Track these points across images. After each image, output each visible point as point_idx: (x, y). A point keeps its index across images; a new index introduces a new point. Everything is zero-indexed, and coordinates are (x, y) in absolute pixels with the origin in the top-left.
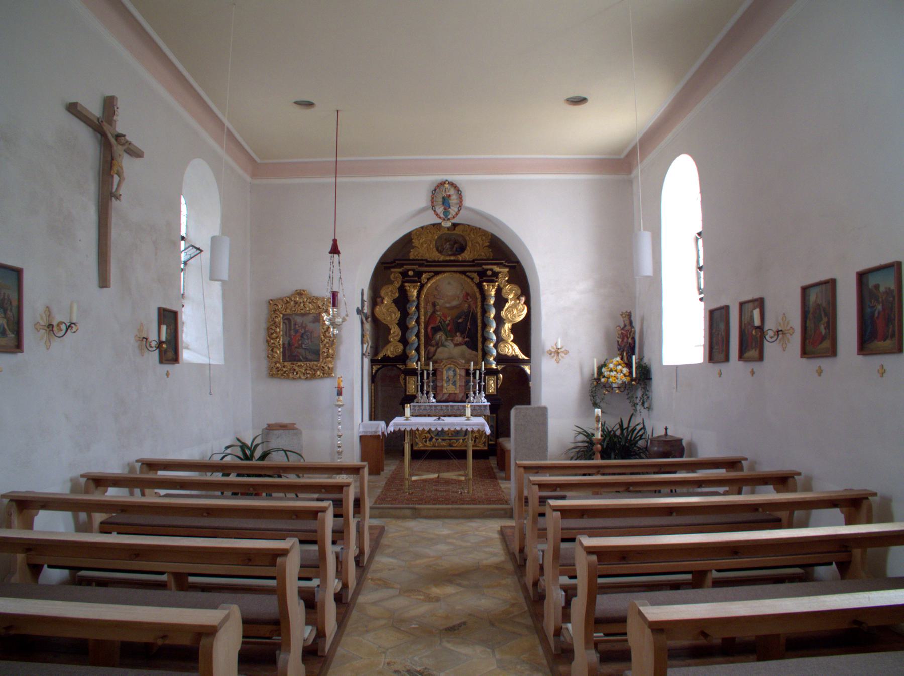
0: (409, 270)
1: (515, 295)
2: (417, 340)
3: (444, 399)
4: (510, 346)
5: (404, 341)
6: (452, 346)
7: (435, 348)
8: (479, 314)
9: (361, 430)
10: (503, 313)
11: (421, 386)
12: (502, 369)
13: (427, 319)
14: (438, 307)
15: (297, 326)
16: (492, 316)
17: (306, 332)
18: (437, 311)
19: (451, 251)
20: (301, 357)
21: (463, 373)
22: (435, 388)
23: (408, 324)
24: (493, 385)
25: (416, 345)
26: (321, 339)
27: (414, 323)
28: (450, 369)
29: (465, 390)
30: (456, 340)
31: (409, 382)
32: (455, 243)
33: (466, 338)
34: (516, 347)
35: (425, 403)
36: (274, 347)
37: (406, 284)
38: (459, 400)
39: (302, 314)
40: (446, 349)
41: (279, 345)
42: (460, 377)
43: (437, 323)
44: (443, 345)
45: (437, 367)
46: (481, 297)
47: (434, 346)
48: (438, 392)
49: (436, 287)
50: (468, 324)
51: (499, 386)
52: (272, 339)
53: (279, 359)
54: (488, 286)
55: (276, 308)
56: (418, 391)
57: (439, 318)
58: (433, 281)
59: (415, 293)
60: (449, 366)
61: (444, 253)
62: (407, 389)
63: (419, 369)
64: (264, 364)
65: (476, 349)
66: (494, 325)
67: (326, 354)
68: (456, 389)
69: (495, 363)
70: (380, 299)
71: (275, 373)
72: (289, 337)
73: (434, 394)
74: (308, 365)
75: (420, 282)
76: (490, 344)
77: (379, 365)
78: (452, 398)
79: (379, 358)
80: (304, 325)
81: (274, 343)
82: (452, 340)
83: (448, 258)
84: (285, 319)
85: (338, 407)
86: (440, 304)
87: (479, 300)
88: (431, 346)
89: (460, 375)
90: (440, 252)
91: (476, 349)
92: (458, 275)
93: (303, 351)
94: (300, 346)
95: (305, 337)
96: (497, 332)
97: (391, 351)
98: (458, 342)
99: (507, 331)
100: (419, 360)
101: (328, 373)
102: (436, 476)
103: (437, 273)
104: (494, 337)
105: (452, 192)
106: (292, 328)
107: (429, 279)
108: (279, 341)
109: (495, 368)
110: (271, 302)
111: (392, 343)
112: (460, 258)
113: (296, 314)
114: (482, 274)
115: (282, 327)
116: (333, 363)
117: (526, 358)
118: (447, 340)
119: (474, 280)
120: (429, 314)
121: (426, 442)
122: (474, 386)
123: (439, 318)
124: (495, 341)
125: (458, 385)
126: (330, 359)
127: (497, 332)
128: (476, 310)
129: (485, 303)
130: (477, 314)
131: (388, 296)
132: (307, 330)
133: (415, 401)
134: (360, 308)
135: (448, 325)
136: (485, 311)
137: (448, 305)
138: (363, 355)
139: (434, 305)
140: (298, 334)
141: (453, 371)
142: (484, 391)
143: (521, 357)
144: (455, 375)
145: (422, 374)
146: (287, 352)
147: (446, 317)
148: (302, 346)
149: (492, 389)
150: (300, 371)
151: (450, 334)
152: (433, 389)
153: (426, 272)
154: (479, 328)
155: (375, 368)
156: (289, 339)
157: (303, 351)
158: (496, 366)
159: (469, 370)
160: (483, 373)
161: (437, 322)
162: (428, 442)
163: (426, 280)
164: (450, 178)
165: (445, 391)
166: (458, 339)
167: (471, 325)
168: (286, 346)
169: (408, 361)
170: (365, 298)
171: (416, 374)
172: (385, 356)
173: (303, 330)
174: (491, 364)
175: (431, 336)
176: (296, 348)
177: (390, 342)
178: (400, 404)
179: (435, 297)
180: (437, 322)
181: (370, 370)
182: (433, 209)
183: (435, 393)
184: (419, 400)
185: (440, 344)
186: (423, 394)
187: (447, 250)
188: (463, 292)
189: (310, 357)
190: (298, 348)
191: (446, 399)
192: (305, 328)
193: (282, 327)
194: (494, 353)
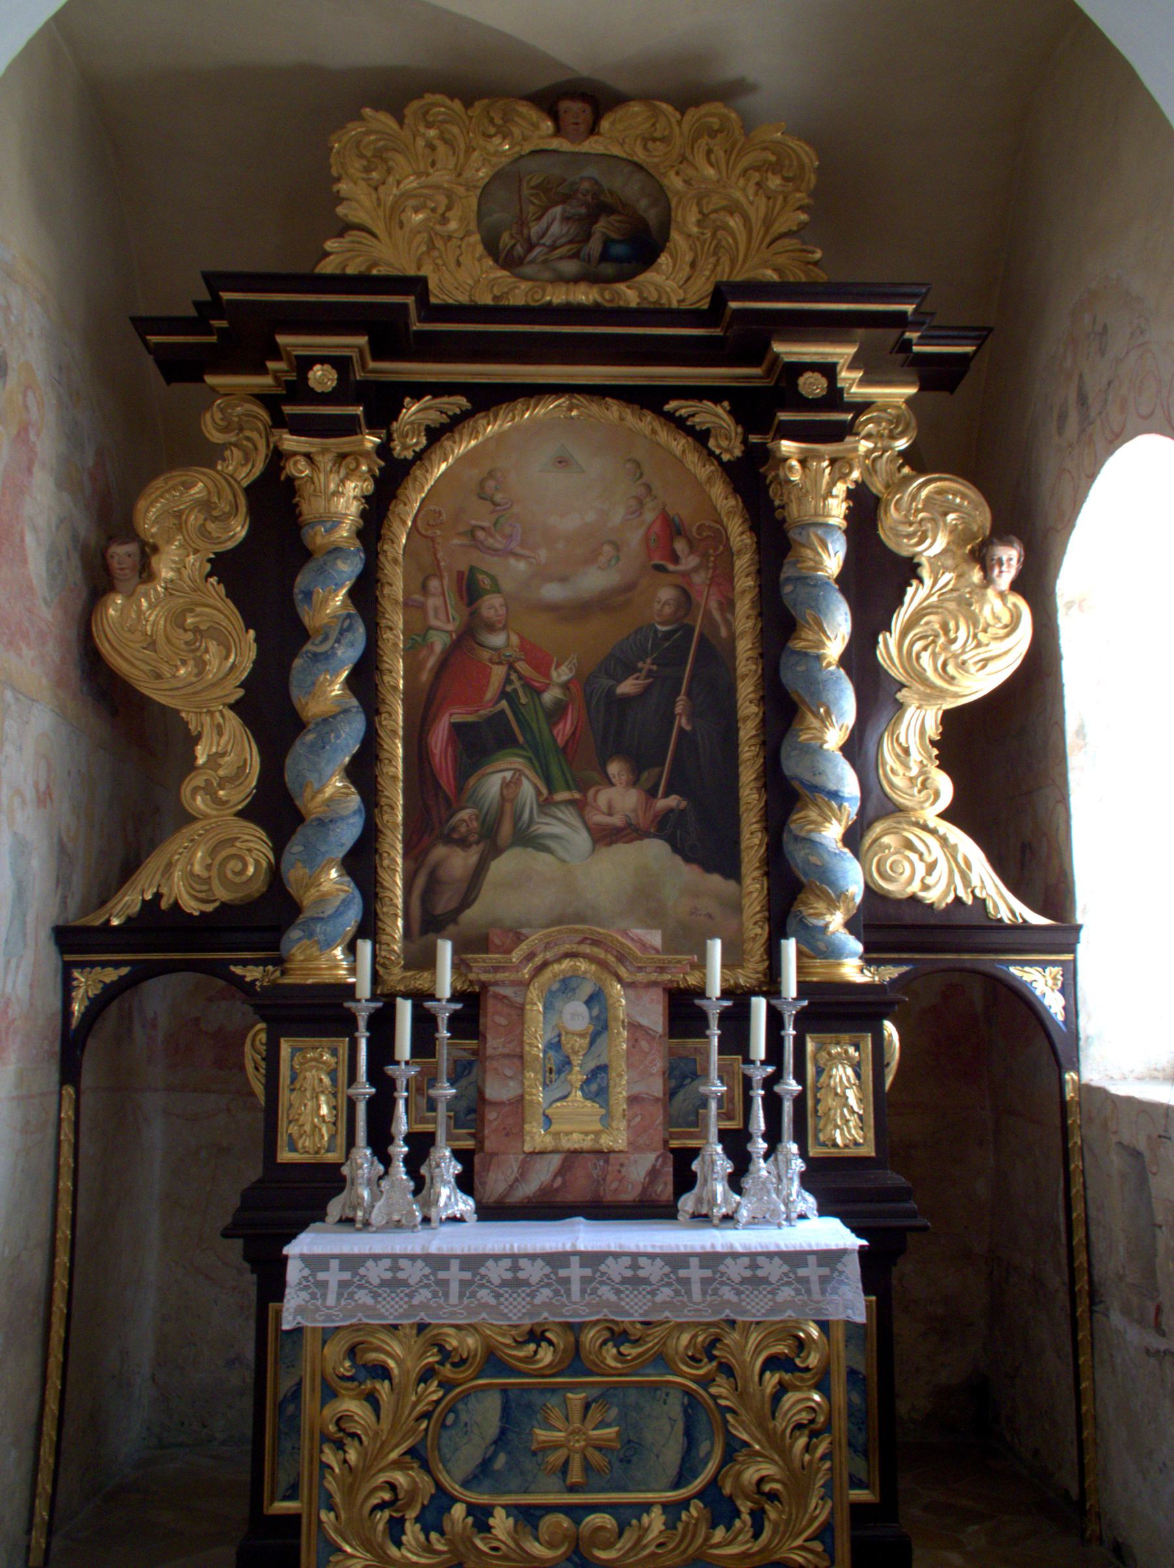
1: (960, 537)
2: (355, 800)
3: (529, 1189)
6: (582, 839)
7: (472, 857)
8: (745, 647)
10: (888, 648)
11: (371, 1103)
13: (425, 677)
14: (491, 606)
18: (491, 628)
19: (576, 256)
21: (654, 1015)
22: (471, 1111)
24: (852, 1096)
25: (348, 833)
27: (336, 690)
28: (567, 986)
29: (670, 1121)
32: (600, 207)
35: (398, 1226)
38: (630, 1194)
40: (541, 862)
42: (634, 1042)
43: (490, 701)
44: (526, 839)
45: (484, 977)
47: (464, 843)
48: (488, 1145)
49: (482, 483)
50: (679, 709)
54: (803, 462)
56: (351, 1143)
57: (498, 673)
58: (463, 446)
60: (566, 964)
61: (528, 270)
62: (282, 1123)
63: (364, 989)
65: (731, 869)
68: (607, 1119)
69: (859, 947)
70: (132, 548)
73: (458, 1154)
77: (117, 965)
78: (579, 1190)
79: (115, 922)
82: (580, 806)
83: (557, 296)
86: (507, 585)
87: (744, 563)
88: (448, 840)
89: (634, 1027)
90: (509, 262)
91: (731, 869)
92: (614, 410)
98: (617, 820)
99: (916, 756)
100: (369, 927)
104: (848, 783)
107: (436, 435)
111: (197, 826)
112: (629, 295)
117: (1036, 919)
118: (546, 804)
119: (712, 444)
120: (439, 642)
121: (396, 1529)
123: (498, 673)
124: (851, 809)
125: (620, 1091)
128: (729, 625)
129: (787, 572)
130: (733, 649)
133: (335, 1208)
135: (557, 712)
137: (553, 592)
141: (589, 1002)
142: (800, 1137)
143: (1005, 916)
144: (601, 1028)
145: (383, 1023)
147: (542, 664)
152: (457, 1121)
153: (418, 390)
154: (747, 731)
155: (87, 985)
159: (701, 993)
161: (491, 693)
163: (418, 441)
165: (537, 1136)
167: (692, 716)
169: (294, 934)
171: (345, 1024)
172: (149, 907)
174: (834, 953)
175: (446, 779)
177: (188, 818)
178: (227, 1234)
179: (477, 545)
180: (491, 693)
183: (469, 1144)
184: (357, 1204)
185: (506, 829)
187: (553, 248)
188: (649, 516)
191: (544, 1191)
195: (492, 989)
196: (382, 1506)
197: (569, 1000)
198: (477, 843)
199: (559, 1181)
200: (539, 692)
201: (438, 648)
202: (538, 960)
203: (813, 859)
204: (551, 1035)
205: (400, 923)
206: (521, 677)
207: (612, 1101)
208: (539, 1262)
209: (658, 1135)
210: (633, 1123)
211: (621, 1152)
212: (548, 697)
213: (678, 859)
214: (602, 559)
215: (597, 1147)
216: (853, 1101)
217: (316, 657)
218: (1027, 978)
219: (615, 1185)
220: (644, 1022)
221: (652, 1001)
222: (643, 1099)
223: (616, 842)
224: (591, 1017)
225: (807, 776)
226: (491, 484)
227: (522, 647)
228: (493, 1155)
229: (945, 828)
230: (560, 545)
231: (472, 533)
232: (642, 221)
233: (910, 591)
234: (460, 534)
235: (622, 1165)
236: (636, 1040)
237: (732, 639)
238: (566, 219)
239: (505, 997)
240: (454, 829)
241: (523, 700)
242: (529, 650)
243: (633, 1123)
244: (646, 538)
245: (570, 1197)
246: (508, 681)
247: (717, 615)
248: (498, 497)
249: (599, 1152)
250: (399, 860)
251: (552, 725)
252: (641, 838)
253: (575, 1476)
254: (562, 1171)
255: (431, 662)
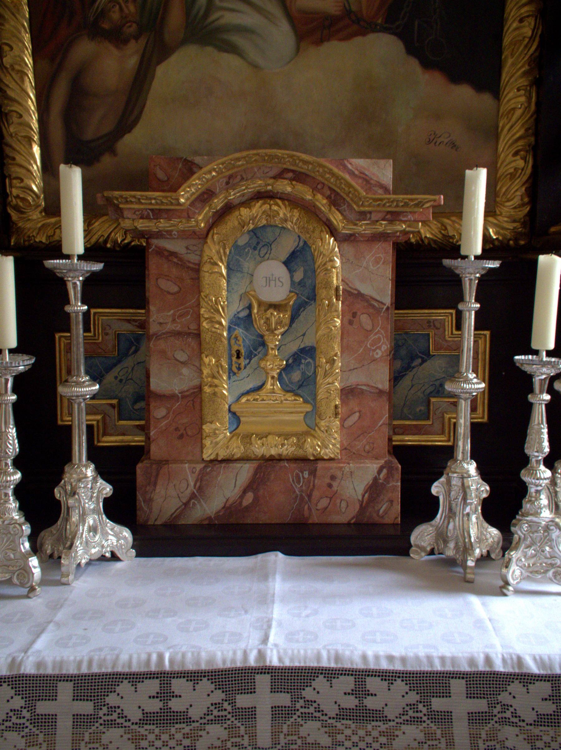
45: (141, 225)
60: (258, 208)
195: (155, 242)
197: (263, 259)
198: (137, 38)
199: (249, 498)
202: (218, 203)
204: (237, 307)
205: (36, 150)
207: (321, 394)
208: (205, 685)
210: (349, 422)
211: (331, 459)
213: (414, 64)
215: (300, 453)
219: (324, 503)
220: (366, 289)
221: (377, 261)
222: (362, 392)
223: (328, 39)
224: (293, 282)
228: (162, 463)
235: (333, 478)
236: (354, 315)
239: (173, 254)
243: (349, 422)
249: (304, 460)
250: (29, 60)
252: (363, 32)
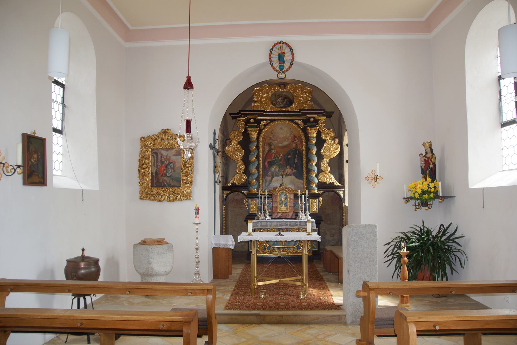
0: (250, 118)
1: (331, 137)
2: (257, 172)
3: (278, 216)
4: (328, 176)
5: (247, 172)
7: (271, 178)
9: (214, 242)
12: (322, 193)
14: (273, 147)
15: (163, 159)
16: (314, 153)
17: (169, 163)
18: (273, 150)
19: (283, 104)
20: (165, 184)
21: (292, 197)
23: (250, 159)
25: (256, 175)
26: (182, 169)
28: (282, 193)
30: (286, 171)
31: (251, 204)
32: (286, 97)
33: (294, 170)
34: (332, 176)
35: (263, 219)
36: (144, 175)
37: (249, 129)
39: (166, 148)
41: (148, 174)
42: (290, 200)
43: (272, 159)
46: (306, 139)
47: (269, 176)
49: (271, 132)
50: (296, 159)
51: (320, 206)
52: (144, 169)
53: (148, 184)
55: (147, 144)
57: (274, 155)
59: (256, 136)
61: (277, 106)
64: (137, 189)
66: (316, 159)
67: (185, 181)
68: (287, 209)
69: (317, 189)
71: (145, 196)
72: (156, 167)
74: (171, 189)
75: (259, 127)
76: (313, 174)
77: (229, 191)
80: (168, 158)
81: (144, 172)
84: (154, 153)
85: (196, 225)
86: (274, 144)
88: (268, 176)
89: (290, 198)
90: (274, 105)
93: (167, 179)
94: (165, 175)
95: (169, 167)
96: (318, 165)
97: (237, 180)
98: (288, 173)
101: (188, 197)
102: (277, 281)
103: (272, 121)
105: (287, 50)
106: (159, 160)
107: (265, 125)
108: (148, 170)
109: (317, 192)
110: (142, 139)
112: (289, 109)
113: (162, 149)
114: (305, 121)
115: (150, 159)
116: (191, 188)
117: (340, 185)
120: (266, 151)
122: (302, 208)
123: (274, 155)
124: (316, 172)
126: (188, 185)
127: (318, 165)
128: (302, 149)
129: (309, 143)
131: (236, 139)
132: (171, 161)
133: (256, 218)
134: (213, 145)
136: (308, 150)
137: (280, 145)
138: (215, 182)
139: (270, 145)
140: (163, 165)
141: (285, 195)
143: (336, 184)
144: (286, 198)
146: (154, 179)
148: (166, 175)
149: (315, 208)
150: (164, 195)
151: (282, 167)
153: (263, 120)
155: (225, 193)
156: (156, 169)
157: (167, 179)
158: (318, 191)
160: (307, 197)
161: (273, 157)
162: (267, 250)
164: (285, 39)
166: (288, 170)
167: (298, 160)
168: (154, 174)
170: (217, 137)
172: (232, 184)
173: (167, 162)
174: (314, 190)
176: (162, 176)
178: (244, 221)
179: (271, 139)
180: (273, 157)
181: (222, 195)
182: (270, 64)
185: (275, 175)
186: (261, 213)
187: (280, 103)
188: (292, 135)
189: (172, 184)
190: (164, 176)
191: (280, 217)
192: (169, 160)
193: (150, 159)
194: (316, 181)
196: (263, 247)
200: (279, 157)
201: (266, 152)
202: (279, 190)
203: (311, 178)
204: (280, 199)
206: (276, 156)
209: (293, 210)
212: (280, 158)
213: (296, 178)
214: (286, 141)
216: (315, 206)
217: (252, 155)
218: (339, 192)
225: (311, 168)
226: (272, 132)
227: (276, 152)
229: (329, 174)
230: (281, 139)
231: (270, 138)
232: (291, 99)
233: (325, 144)
234: (269, 138)
237: (302, 150)
238: (281, 99)
240: (269, 174)
241: (276, 158)
242: (278, 153)
244: (292, 138)
245: (283, 218)
246: (275, 156)
247: (300, 147)
248: (273, 133)
249: (286, 212)
251: (280, 161)
252: (291, 175)
253: (283, 244)
254: (281, 215)
255: (265, 154)
